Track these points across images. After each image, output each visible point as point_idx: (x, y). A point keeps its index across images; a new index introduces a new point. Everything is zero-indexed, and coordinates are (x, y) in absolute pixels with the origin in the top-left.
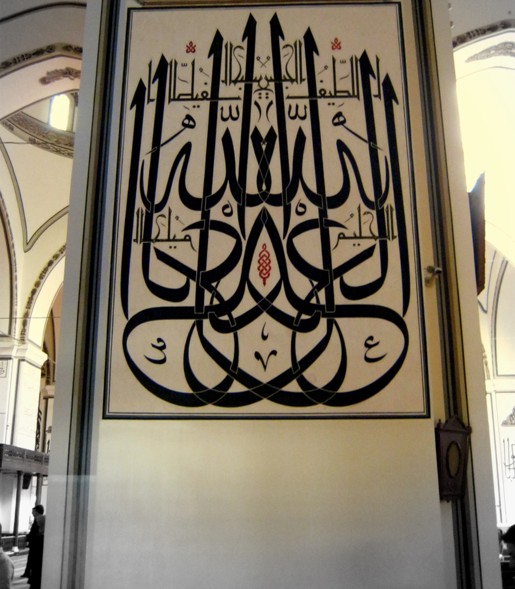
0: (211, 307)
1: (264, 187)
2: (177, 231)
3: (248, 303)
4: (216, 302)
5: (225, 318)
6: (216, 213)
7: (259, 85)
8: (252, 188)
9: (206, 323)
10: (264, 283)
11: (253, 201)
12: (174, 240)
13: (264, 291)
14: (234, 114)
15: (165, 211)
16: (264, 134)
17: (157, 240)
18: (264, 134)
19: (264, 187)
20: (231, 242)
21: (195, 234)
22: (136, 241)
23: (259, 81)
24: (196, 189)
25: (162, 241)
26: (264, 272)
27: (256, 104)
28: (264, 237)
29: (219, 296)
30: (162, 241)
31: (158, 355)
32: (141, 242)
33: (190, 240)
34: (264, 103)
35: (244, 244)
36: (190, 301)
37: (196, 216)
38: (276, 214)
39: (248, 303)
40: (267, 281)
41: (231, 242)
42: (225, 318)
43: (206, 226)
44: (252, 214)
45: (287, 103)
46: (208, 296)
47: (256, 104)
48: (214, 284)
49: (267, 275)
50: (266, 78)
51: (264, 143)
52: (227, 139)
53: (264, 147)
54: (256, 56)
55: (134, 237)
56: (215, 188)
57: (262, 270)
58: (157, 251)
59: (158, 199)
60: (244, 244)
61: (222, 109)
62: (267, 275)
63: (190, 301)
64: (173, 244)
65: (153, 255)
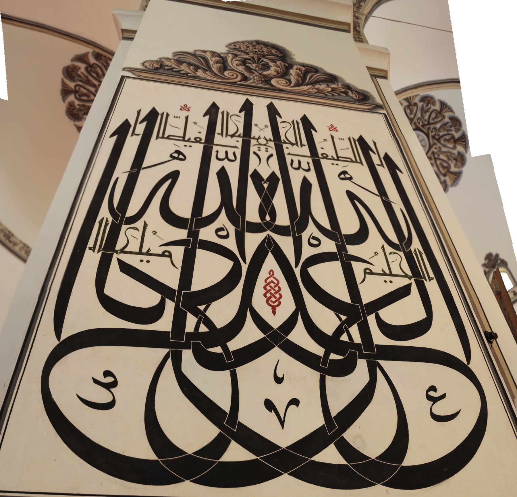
0: (196, 334)
1: (268, 218)
2: (152, 243)
3: (250, 334)
4: (203, 328)
5: (218, 350)
6: (207, 234)
7: (258, 141)
8: (252, 215)
9: (187, 355)
10: (274, 313)
11: (255, 228)
12: (148, 253)
13: (275, 322)
14: (231, 157)
15: (139, 224)
16: (265, 176)
17: (123, 251)
18: (265, 176)
19: (268, 218)
20: (228, 264)
21: (178, 252)
22: (93, 249)
23: (258, 139)
25: (131, 253)
26: (273, 299)
27: (255, 153)
29: (208, 323)
30: (131, 253)
31: (102, 396)
32: (99, 251)
33: (170, 256)
34: (264, 155)
35: (245, 268)
36: (165, 324)
37: (182, 234)
39: (250, 334)
40: (278, 309)
41: (228, 264)
42: (218, 350)
43: (192, 246)
44: (253, 241)
45: (288, 159)
46: (191, 321)
47: (255, 153)
48: (202, 308)
49: (277, 303)
50: (265, 138)
51: (265, 182)
52: (222, 174)
53: (266, 186)
54: (254, 122)
55: (91, 244)
56: (208, 210)
57: (270, 297)
58: (120, 262)
59: (131, 212)
60: (245, 268)
61: (217, 152)
62: (277, 303)
63: (165, 324)
64: (145, 258)
65: (114, 266)
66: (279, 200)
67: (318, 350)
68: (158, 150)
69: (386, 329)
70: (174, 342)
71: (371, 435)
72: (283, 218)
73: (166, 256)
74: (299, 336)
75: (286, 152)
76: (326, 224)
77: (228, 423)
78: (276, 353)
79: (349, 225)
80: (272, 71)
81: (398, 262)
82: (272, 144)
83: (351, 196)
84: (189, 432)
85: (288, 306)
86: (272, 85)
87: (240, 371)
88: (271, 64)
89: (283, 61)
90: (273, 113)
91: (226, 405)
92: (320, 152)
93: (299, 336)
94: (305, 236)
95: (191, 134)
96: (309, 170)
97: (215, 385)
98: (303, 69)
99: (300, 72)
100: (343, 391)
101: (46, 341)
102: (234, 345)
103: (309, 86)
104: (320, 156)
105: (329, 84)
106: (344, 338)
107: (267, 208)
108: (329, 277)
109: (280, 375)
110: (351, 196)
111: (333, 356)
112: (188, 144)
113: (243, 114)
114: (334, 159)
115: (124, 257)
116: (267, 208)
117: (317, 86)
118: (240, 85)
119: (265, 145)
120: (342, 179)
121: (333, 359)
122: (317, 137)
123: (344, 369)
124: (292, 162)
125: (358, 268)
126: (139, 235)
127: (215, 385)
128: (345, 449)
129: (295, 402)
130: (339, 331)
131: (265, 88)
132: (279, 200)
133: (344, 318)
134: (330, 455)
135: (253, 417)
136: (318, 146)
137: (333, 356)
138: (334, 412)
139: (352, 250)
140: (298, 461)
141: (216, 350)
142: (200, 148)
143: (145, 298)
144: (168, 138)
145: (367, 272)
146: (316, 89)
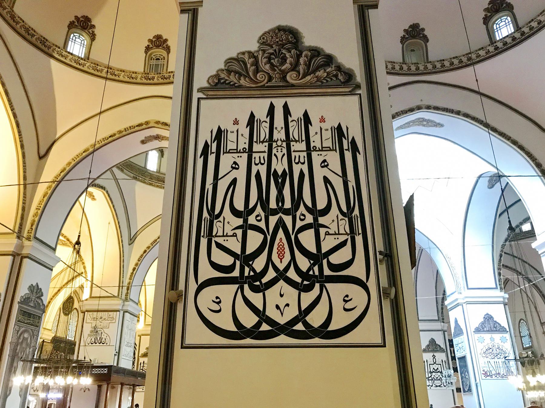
0: (249, 277)
1: (280, 204)
2: (228, 230)
3: (271, 274)
4: (252, 273)
5: (258, 283)
6: (252, 220)
8: (273, 205)
9: (246, 286)
10: (281, 262)
11: (274, 212)
12: (227, 236)
13: (281, 267)
15: (221, 219)
16: (280, 174)
17: (216, 236)
18: (280, 174)
19: (280, 204)
21: (239, 232)
22: (203, 236)
23: (276, 142)
24: (240, 205)
25: (219, 236)
26: (281, 255)
27: (275, 155)
28: (281, 234)
29: (254, 270)
30: (219, 236)
33: (236, 236)
34: (279, 155)
35: (269, 238)
36: (236, 273)
37: (240, 222)
38: (288, 220)
39: (271, 274)
42: (258, 283)
43: (245, 227)
44: (273, 220)
45: (293, 154)
46: (247, 269)
47: (275, 155)
48: (251, 263)
52: (258, 175)
53: (280, 180)
55: (202, 234)
58: (216, 242)
59: (217, 212)
60: (269, 238)
61: (255, 158)
64: (226, 238)
67: (298, 280)
68: (226, 161)
70: (239, 281)
72: (288, 204)
73: (235, 236)
74: (292, 274)
75: (293, 149)
76: (310, 204)
78: (281, 283)
79: (321, 204)
80: (287, 66)
82: (284, 144)
83: (326, 180)
85: (287, 257)
86: (287, 82)
87: (267, 292)
88: (288, 55)
89: (296, 50)
91: (261, 308)
92: (312, 144)
93: (292, 274)
94: (298, 214)
95: (240, 147)
96: (303, 163)
97: (256, 299)
98: (309, 54)
99: (307, 60)
100: (308, 298)
102: (265, 280)
103: (312, 75)
104: (312, 149)
105: (326, 68)
106: (311, 273)
107: (280, 198)
108: (307, 239)
109: (282, 293)
110: (326, 180)
111: (305, 283)
112: (239, 155)
113: (268, 120)
114: (319, 150)
115: (217, 239)
116: (280, 198)
117: (318, 73)
118: (267, 87)
119: (280, 146)
120: (322, 167)
122: (312, 130)
123: (308, 289)
124: (295, 157)
125: (322, 231)
126: (221, 225)
127: (256, 299)
128: (306, 324)
129: (287, 305)
130: (309, 270)
131: (283, 86)
133: (312, 262)
134: (300, 327)
135: (272, 313)
136: (312, 139)
137: (305, 283)
138: (303, 308)
139: (321, 220)
142: (245, 156)
144: (229, 152)
145: (327, 234)
146: (316, 77)
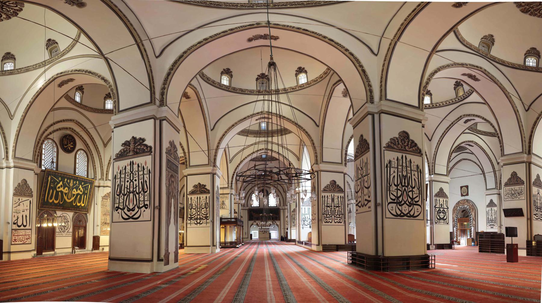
3: (403, 202)
6: (399, 188)
11: (403, 186)
37: (396, 188)
38: (406, 188)
39: (403, 202)
43: (397, 189)
44: (403, 188)
66: (406, 181)
69: (416, 202)
71: (412, 213)
72: (406, 185)
74: (407, 202)
77: (402, 212)
79: (413, 186)
81: (418, 191)
84: (399, 213)
90: (406, 158)
93: (407, 202)
97: (400, 208)
101: (387, 204)
108: (410, 194)
121: (410, 205)
122: (412, 165)
123: (410, 206)
127: (400, 208)
132: (406, 181)
135: (403, 211)
140: (406, 215)
141: (399, 204)
143: (394, 198)
